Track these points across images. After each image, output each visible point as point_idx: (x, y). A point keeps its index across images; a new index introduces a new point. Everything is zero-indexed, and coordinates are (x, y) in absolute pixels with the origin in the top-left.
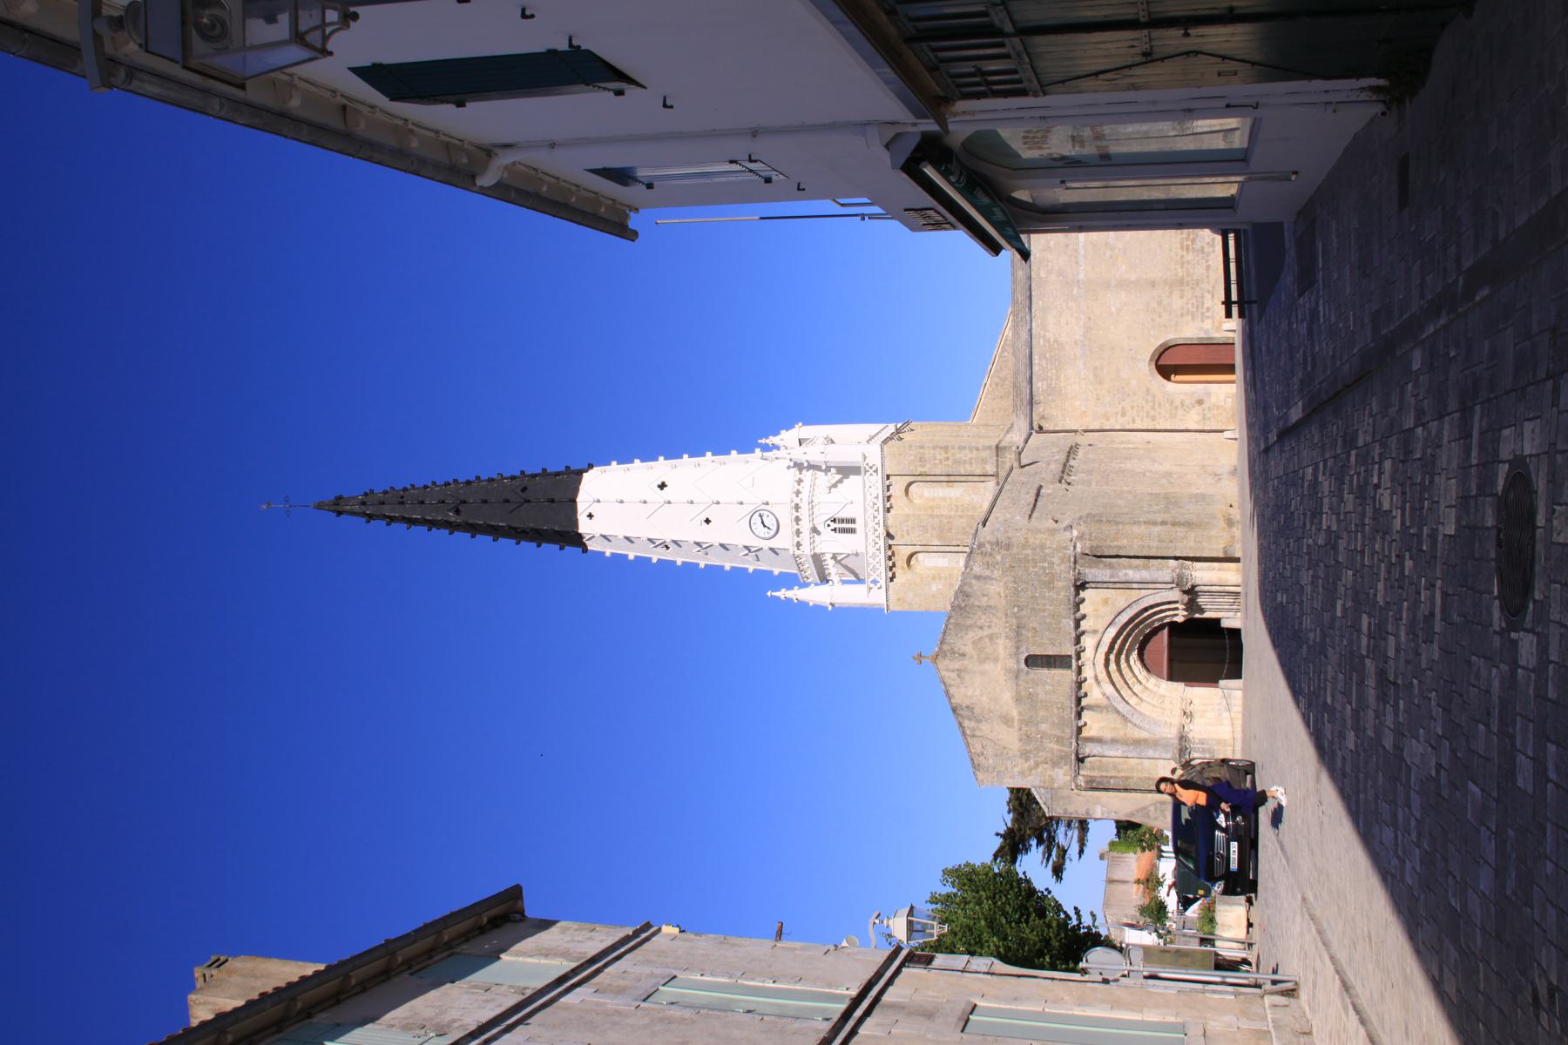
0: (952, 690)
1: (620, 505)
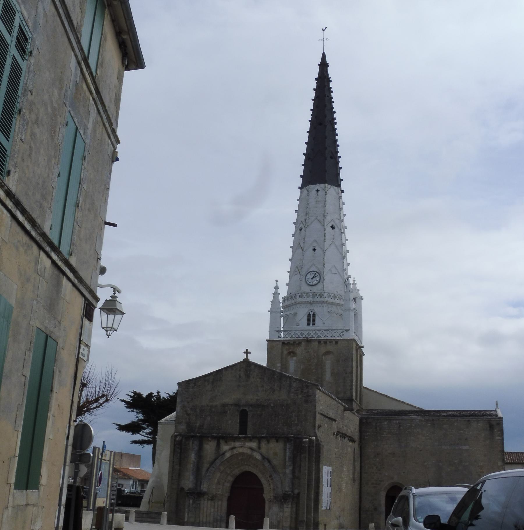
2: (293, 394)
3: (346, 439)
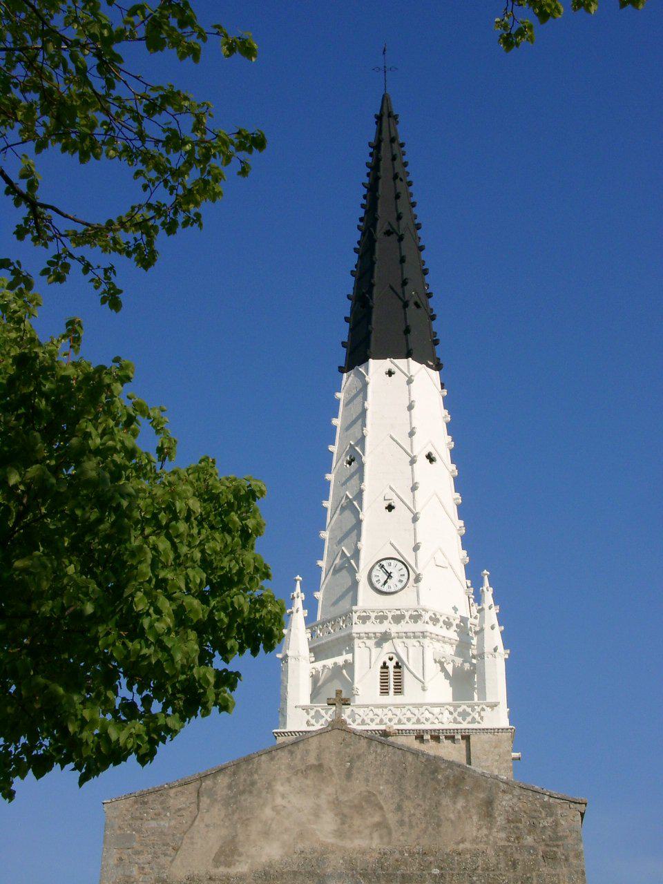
0: (283, 756)
2: (503, 835)
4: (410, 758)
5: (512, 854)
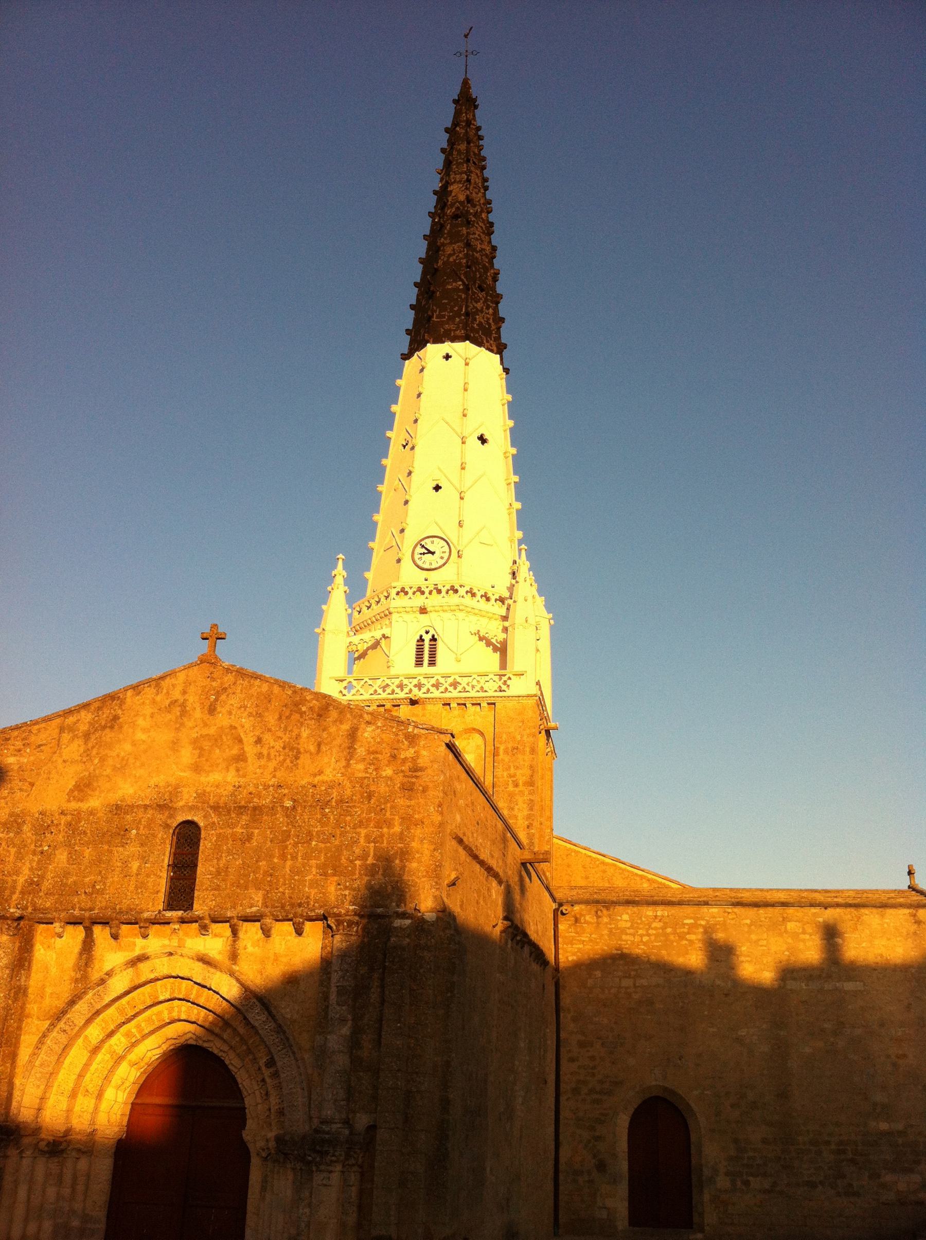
0: (149, 692)
1: (457, 397)
2: (361, 766)
3: (527, 949)
4: (276, 690)
5: (368, 785)
